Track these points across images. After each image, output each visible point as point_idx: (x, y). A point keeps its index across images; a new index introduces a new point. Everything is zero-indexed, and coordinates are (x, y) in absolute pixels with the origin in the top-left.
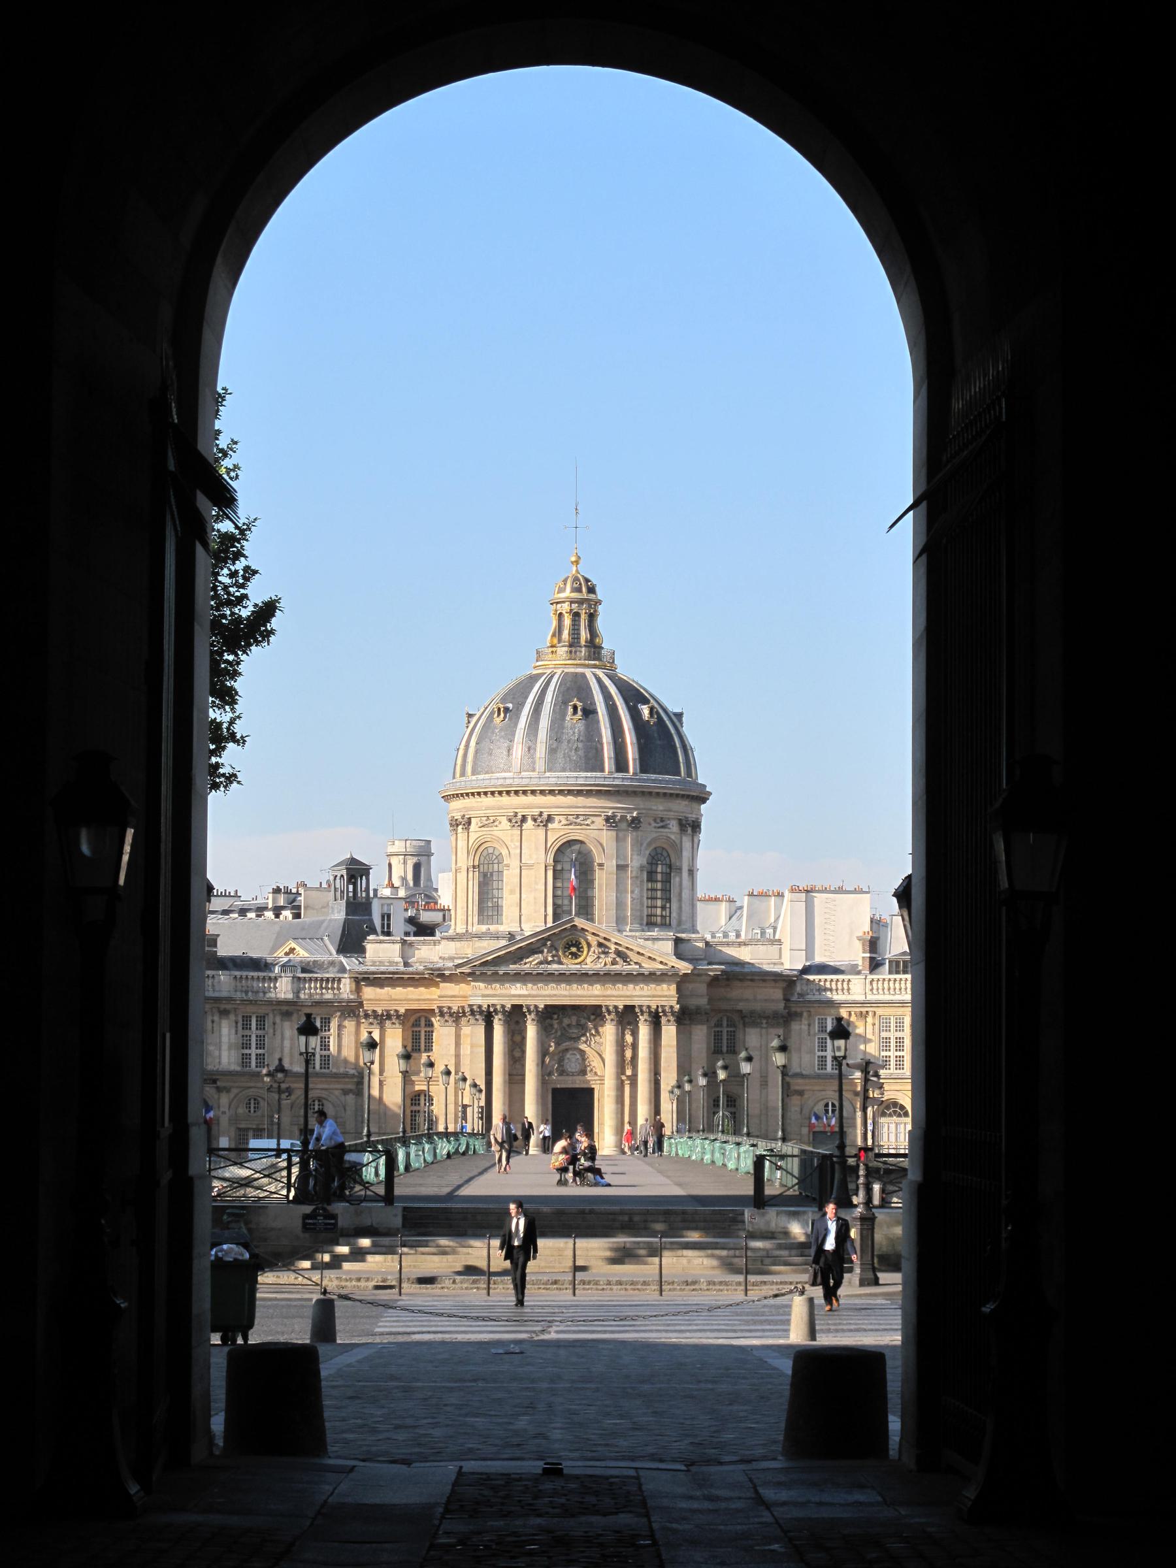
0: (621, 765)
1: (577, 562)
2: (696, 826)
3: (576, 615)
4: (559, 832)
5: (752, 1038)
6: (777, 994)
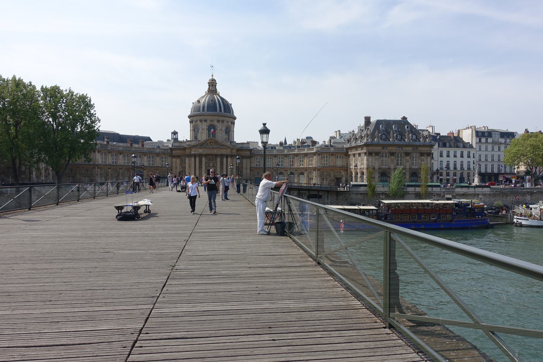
0: (221, 111)
1: (212, 76)
2: (234, 123)
3: (212, 85)
4: (209, 123)
5: (244, 161)
6: (249, 153)
